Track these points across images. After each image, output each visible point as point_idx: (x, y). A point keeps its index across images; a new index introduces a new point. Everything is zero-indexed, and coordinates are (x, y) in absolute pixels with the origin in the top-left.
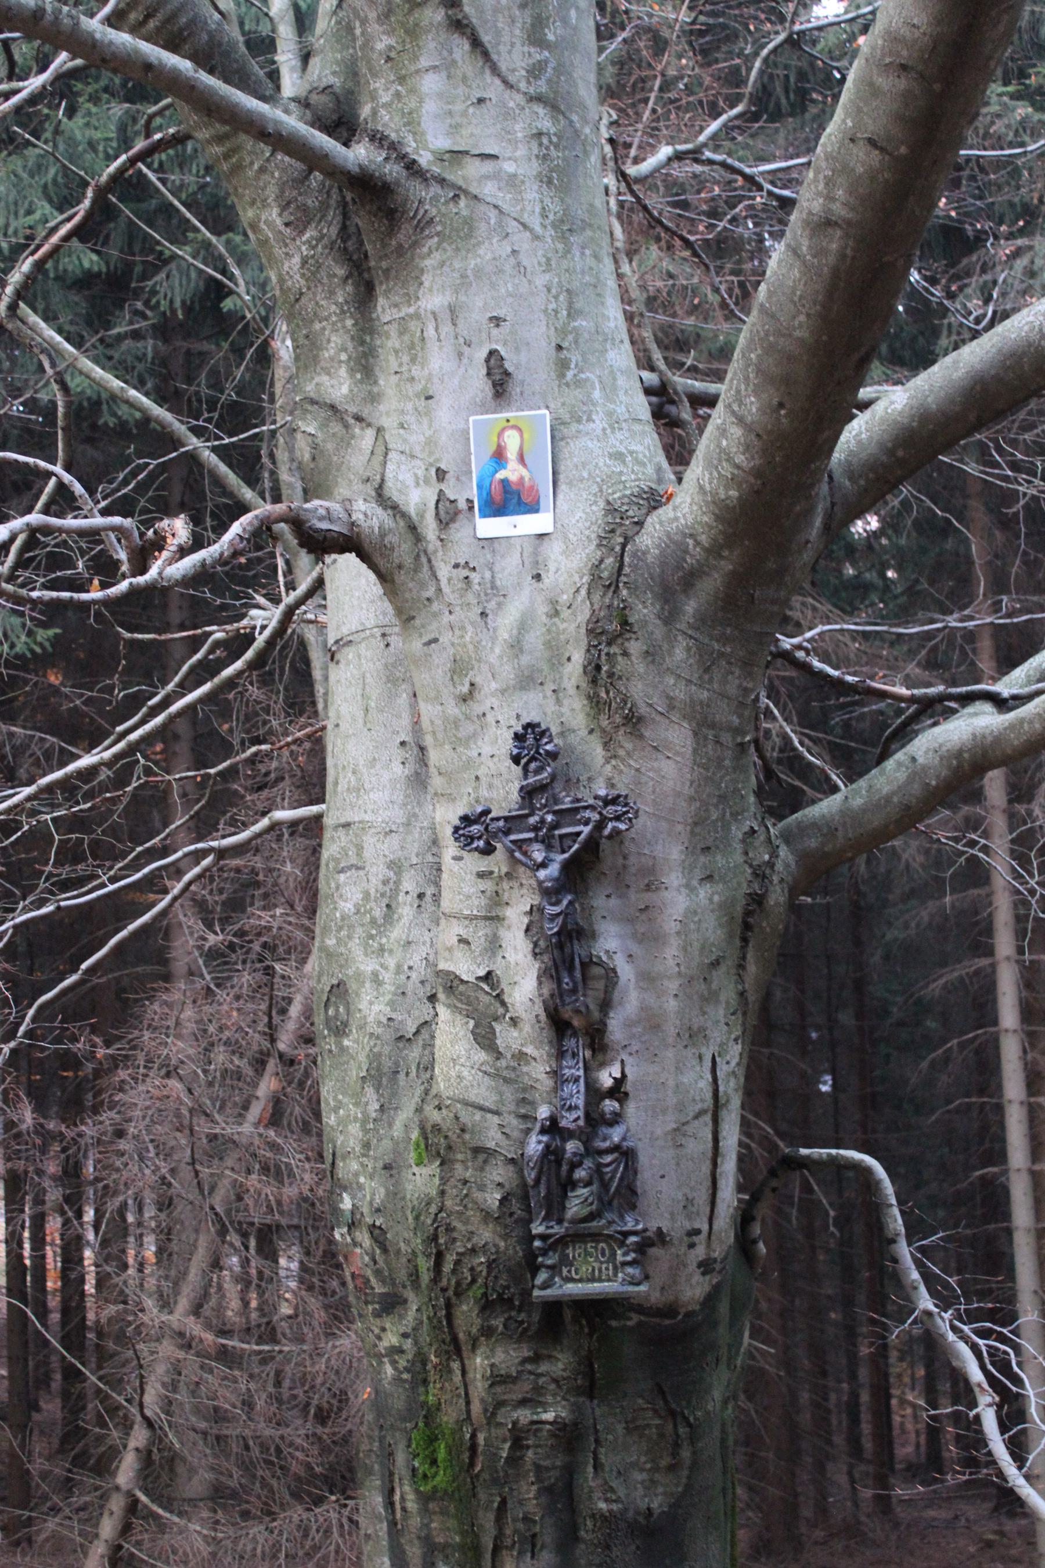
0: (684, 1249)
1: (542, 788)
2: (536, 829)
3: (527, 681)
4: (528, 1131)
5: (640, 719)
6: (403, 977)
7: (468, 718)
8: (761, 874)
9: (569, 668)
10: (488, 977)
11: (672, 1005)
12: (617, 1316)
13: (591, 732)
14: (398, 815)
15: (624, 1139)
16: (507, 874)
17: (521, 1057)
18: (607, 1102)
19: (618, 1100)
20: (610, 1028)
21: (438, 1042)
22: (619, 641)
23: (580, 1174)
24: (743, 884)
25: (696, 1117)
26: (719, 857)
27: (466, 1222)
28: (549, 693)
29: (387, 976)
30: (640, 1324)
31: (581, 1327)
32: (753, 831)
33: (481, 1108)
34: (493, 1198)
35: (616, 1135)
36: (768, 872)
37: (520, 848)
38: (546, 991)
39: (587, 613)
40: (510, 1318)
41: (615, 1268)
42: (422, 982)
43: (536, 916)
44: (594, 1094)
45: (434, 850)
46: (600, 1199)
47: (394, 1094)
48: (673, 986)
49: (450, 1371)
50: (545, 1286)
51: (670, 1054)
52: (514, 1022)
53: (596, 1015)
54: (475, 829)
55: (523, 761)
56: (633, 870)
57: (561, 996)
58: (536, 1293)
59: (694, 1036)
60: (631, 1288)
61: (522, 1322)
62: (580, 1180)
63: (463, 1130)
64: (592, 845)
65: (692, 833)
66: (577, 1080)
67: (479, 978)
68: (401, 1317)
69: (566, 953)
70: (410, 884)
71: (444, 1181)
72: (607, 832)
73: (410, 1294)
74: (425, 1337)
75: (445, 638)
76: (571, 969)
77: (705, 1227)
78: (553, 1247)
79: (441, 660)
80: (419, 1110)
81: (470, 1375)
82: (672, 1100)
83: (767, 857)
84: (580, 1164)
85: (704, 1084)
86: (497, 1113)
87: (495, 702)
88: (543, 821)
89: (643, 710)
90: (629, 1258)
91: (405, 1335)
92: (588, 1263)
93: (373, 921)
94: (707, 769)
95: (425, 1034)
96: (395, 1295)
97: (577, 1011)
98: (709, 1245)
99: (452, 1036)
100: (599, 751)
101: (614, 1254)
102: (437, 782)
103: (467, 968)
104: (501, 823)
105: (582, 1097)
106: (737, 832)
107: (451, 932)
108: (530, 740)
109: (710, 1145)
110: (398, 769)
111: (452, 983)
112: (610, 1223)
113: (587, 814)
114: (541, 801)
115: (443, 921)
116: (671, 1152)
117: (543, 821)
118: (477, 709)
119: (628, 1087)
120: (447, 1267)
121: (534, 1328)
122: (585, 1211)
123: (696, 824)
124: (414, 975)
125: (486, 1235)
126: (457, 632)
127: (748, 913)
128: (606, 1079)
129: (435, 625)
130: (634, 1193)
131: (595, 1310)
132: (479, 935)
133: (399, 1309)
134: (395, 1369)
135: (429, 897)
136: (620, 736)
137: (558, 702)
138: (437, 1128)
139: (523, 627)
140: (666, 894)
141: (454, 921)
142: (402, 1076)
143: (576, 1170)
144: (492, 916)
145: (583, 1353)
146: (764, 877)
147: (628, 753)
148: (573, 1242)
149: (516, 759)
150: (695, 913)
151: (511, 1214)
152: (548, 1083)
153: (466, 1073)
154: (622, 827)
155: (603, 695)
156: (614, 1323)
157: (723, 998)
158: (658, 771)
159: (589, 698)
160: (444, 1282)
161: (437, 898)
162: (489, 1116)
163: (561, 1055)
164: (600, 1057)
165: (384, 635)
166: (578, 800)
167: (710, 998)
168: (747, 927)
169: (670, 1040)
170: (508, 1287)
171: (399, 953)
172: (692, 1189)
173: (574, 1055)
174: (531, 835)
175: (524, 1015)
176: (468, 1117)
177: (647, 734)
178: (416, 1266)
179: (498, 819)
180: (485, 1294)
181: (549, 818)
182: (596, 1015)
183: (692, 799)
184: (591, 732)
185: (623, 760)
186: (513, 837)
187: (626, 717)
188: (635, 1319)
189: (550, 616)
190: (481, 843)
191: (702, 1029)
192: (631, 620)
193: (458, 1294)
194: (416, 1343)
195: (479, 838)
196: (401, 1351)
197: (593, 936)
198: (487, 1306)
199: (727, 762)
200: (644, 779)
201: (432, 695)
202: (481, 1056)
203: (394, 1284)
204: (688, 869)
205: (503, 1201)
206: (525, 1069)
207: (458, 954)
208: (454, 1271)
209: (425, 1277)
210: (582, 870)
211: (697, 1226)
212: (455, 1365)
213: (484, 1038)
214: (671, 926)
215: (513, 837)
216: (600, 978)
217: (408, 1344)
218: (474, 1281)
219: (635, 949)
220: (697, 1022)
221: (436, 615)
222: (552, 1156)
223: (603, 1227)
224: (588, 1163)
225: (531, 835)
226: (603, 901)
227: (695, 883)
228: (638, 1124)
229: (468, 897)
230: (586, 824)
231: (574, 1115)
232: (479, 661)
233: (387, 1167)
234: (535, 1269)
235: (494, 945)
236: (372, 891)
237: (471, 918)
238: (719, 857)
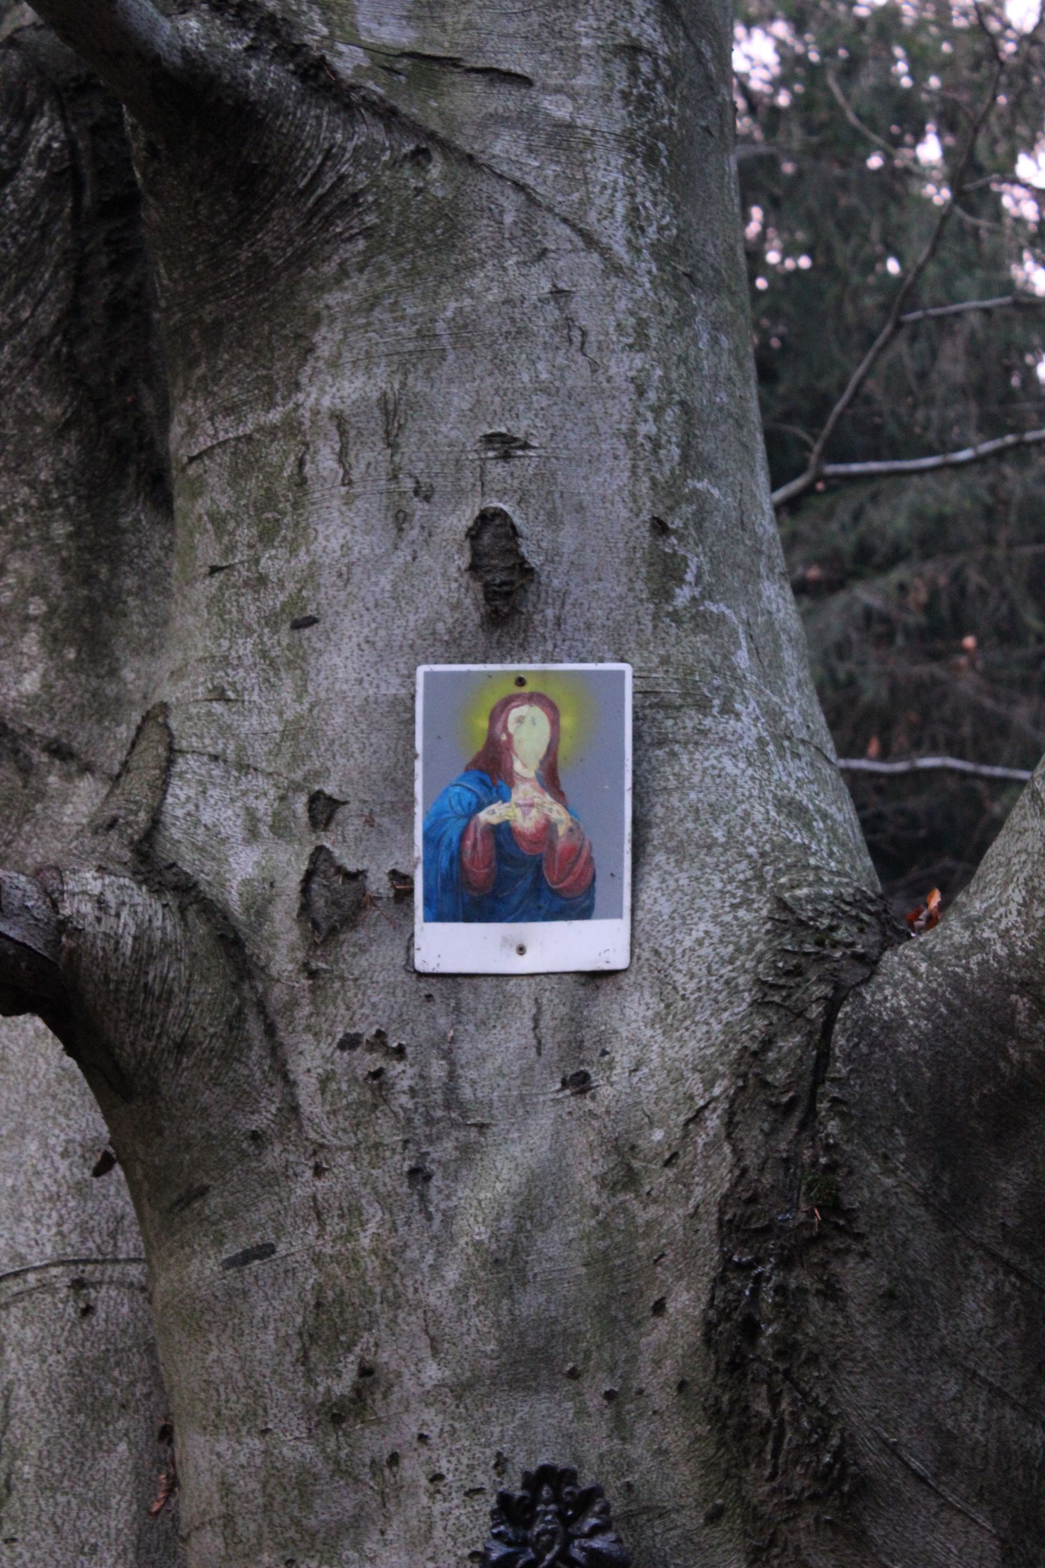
3: (531, 1363)
5: (864, 1485)
7: (342, 1469)
9: (659, 1332)
13: (714, 1517)
22: (816, 1255)
28: (594, 1402)
39: (724, 1175)
75: (294, 1246)
79: (275, 1309)
87: (433, 1420)
89: (872, 1459)
118: (374, 1444)
126: (335, 1226)
129: (267, 1207)
137: (621, 1428)
139: (530, 1210)
155: (761, 1407)
159: (716, 1415)
165: (78, 1285)
177: (876, 1533)
187: (822, 1476)
189: (609, 1185)
192: (850, 1200)
201: (237, 1405)
221: (271, 1181)
232: (395, 1303)
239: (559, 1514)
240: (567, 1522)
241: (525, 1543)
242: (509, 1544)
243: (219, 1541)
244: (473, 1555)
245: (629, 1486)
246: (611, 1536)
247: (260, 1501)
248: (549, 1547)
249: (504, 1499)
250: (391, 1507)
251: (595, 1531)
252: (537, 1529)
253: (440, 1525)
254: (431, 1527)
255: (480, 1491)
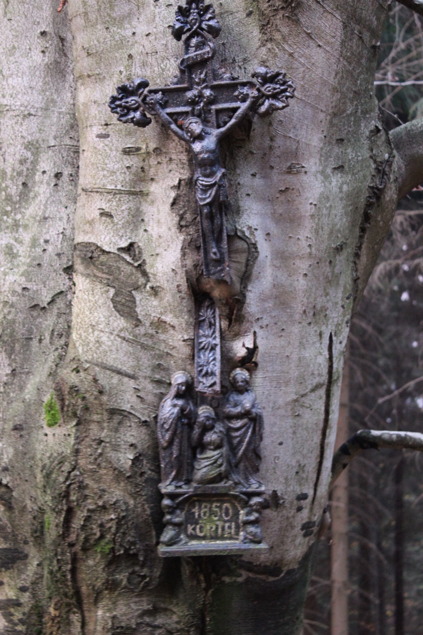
0: (293, 511)
1: (202, 63)
2: (193, 103)
4: (161, 396)
6: (39, 250)
8: (382, 170)
10: (130, 248)
11: (301, 283)
12: (231, 573)
13: (249, 14)
14: (36, 100)
15: (253, 406)
16: (155, 150)
17: (159, 325)
18: (238, 371)
19: (248, 370)
20: (248, 301)
21: (75, 310)
23: (211, 437)
24: (366, 178)
25: (313, 390)
26: (349, 150)
27: (98, 481)
29: (21, 250)
30: (248, 580)
31: (199, 582)
32: (377, 130)
33: (119, 372)
34: (126, 458)
35: (246, 401)
36: (387, 169)
37: (176, 122)
38: (189, 262)
40: (133, 573)
41: (238, 527)
42: (59, 255)
43: (184, 190)
44: (229, 363)
45: (72, 134)
46: (229, 462)
47: (26, 360)
48: (303, 266)
49: (69, 623)
50: (170, 543)
51: (296, 329)
52: (155, 291)
53: (238, 286)
54: (132, 100)
55: (184, 37)
56: (278, 152)
57: (207, 266)
58: (162, 549)
59: (317, 314)
60: (252, 546)
61: (144, 577)
62: (210, 443)
63: (101, 392)
64: (245, 124)
65: (331, 122)
66: (213, 348)
67: (120, 249)
68: (20, 572)
69: (211, 226)
70: (47, 164)
71: (79, 440)
72: (263, 109)
73: (32, 550)
74: (44, 591)
76: (218, 241)
77: (311, 493)
78: (180, 506)
80: (52, 374)
81: (90, 627)
82: (294, 373)
83: (387, 156)
84: (212, 427)
85: (322, 360)
86: (132, 377)
88: (201, 95)
90: (252, 518)
91: (23, 589)
92: (212, 521)
93: (9, 199)
94: (350, 63)
95: (60, 303)
96: (16, 550)
97: (221, 282)
98: (311, 509)
99: (90, 304)
100: (256, 33)
101: (237, 514)
102: (82, 64)
103: (109, 239)
104: (159, 96)
105: (218, 364)
106: (365, 129)
107: (91, 208)
108: (193, 15)
109: (322, 417)
110: (37, 58)
111: (92, 255)
112: (236, 484)
113: (245, 90)
114: (199, 76)
115: (83, 198)
116: (290, 421)
117: (201, 95)
119: (258, 358)
120: (77, 523)
121: (155, 582)
122: (214, 472)
123: (335, 115)
124: (50, 248)
125: (117, 493)
127: (369, 205)
128: (239, 349)
130: (258, 457)
131: (212, 565)
132: (122, 208)
133: (19, 564)
134: (10, 621)
135: (67, 176)
136: (278, 20)
138: (74, 390)
140: (305, 178)
141: (97, 196)
142: (35, 343)
143: (206, 433)
144: (137, 190)
145: (198, 607)
146: (384, 173)
147: (284, 38)
148: (200, 502)
149: (177, 34)
150: (327, 199)
151: (142, 474)
152: (186, 350)
153: (104, 339)
154: (280, 104)
156: (227, 579)
157: (342, 282)
158: (308, 58)
160: (73, 537)
161: (74, 178)
162: (126, 379)
163: (198, 324)
164: (236, 328)
166: (234, 79)
167: (331, 281)
168: (367, 217)
169: (297, 317)
170: (133, 543)
171: (34, 229)
172: (304, 457)
173: (211, 325)
174: (188, 109)
175: (165, 285)
176: (107, 380)
177: (302, 20)
178: (42, 524)
179: (156, 92)
180: (113, 550)
181: (207, 93)
182: (238, 286)
183: (335, 90)
184: (249, 14)
185: (278, 44)
186: (169, 110)
188: (244, 576)
190: (138, 115)
191: (324, 309)
193: (85, 549)
194: (34, 596)
195: (135, 110)
196: (17, 604)
197: (238, 211)
198: (113, 561)
199: (363, 61)
200: (296, 65)
202: (121, 323)
203: (15, 541)
204: (325, 157)
205: (136, 460)
206: (162, 337)
207: (100, 227)
208: (83, 527)
209: (52, 533)
210: (233, 146)
211: (305, 491)
212: (75, 618)
213: (125, 306)
214: (307, 209)
215: (169, 110)
216: (243, 252)
217: (25, 598)
218: (102, 537)
219: (274, 229)
220: (320, 302)
222: (185, 419)
223: (230, 488)
224: (219, 427)
225: (188, 109)
226: (249, 180)
227: (329, 171)
228: (263, 394)
229: (113, 173)
230: (243, 100)
231: (209, 381)
233: (16, 428)
234: (160, 527)
235: (137, 219)
236: (9, 171)
237: (115, 193)
238: (349, 150)
239: (198, 13)
240: (201, 16)
241: (187, 23)
242: (182, 23)
243: (83, 21)
244: (169, 26)
245: (221, 4)
246: (215, 21)
247: (97, 8)
248: (195, 24)
249: (180, 8)
250: (141, 10)
251: (210, 19)
252: (191, 18)
253: (158, 16)
254: (155, 17)
255: (171, 5)
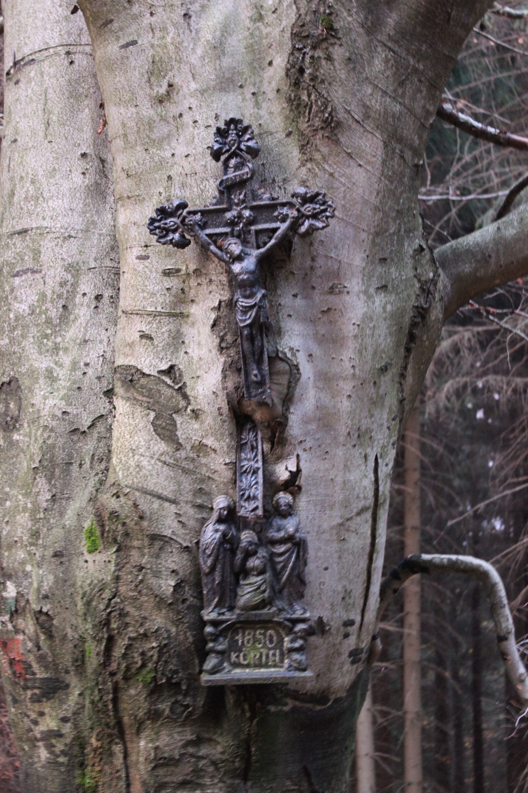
0: (340, 638)
1: (241, 184)
2: (232, 223)
3: (227, 82)
4: (203, 522)
5: (339, 124)
6: (79, 373)
7: (163, 119)
8: (426, 289)
9: (270, 72)
10: (170, 371)
11: (345, 405)
12: (276, 702)
13: (289, 134)
14: (77, 222)
15: (297, 530)
16: (195, 271)
17: (201, 448)
18: (281, 494)
19: (292, 494)
20: (290, 423)
21: (115, 434)
22: (324, 45)
23: (254, 562)
24: (411, 297)
25: (359, 514)
26: (393, 270)
27: (139, 608)
28: (249, 96)
29: (61, 373)
30: (294, 710)
31: (243, 712)
32: (422, 249)
33: (160, 497)
34: (167, 585)
35: (290, 525)
36: (432, 288)
37: (215, 243)
38: (230, 385)
39: (293, 17)
40: (176, 702)
41: (282, 655)
42: (99, 378)
43: (224, 311)
44: (271, 486)
45: (113, 255)
46: (272, 588)
47: (66, 485)
48: (347, 387)
49: (111, 754)
50: (214, 671)
51: (340, 452)
52: (196, 414)
53: (279, 408)
54: (171, 221)
55: (223, 158)
56: (319, 272)
57: (248, 388)
58: (205, 677)
59: (362, 436)
60: (297, 674)
61: (187, 706)
62: (253, 569)
63: (141, 518)
64: (285, 244)
65: (373, 241)
66: (255, 472)
67: (160, 372)
68: (62, 702)
69: (252, 347)
70: (87, 286)
71: (119, 566)
72: (303, 229)
73: (73, 680)
74: (86, 722)
75: (145, 40)
76: (259, 362)
77: (358, 619)
78: (223, 633)
79: (139, 62)
80: (92, 500)
81: (133, 758)
82: (339, 496)
83: (431, 275)
84: (255, 553)
85: (368, 482)
86: (173, 502)
87: (194, 102)
88: (240, 216)
89: (341, 115)
90: (297, 645)
91: (64, 720)
92: (256, 649)
93: (49, 321)
94: (392, 182)
95: (101, 427)
96: (57, 680)
97: (262, 404)
98: (359, 636)
99: (131, 428)
100: (296, 153)
101: (281, 641)
102: (122, 185)
103: (149, 362)
104: (198, 217)
105: (260, 488)
106: (409, 248)
107: (131, 330)
108: (232, 136)
109: (369, 541)
110: (78, 179)
111: (132, 378)
112: (280, 610)
113: (285, 211)
114: (238, 197)
115: (123, 320)
116: (335, 546)
117: (240, 216)
118: (173, 110)
119: (302, 481)
120: (118, 651)
121: (199, 712)
122: (258, 598)
123: (377, 234)
124: (90, 371)
125: (159, 620)
126: (158, 34)
127: (414, 325)
128: (282, 472)
129: (134, 27)
130: (303, 582)
131: (258, 695)
132: (162, 330)
133: (60, 694)
134: (52, 753)
135: (107, 299)
136: (318, 140)
137: (257, 105)
138: (114, 515)
139: (226, 30)
140: (347, 298)
141: (137, 318)
142: (75, 467)
144: (177, 312)
145: (243, 737)
146: (429, 292)
147: (324, 158)
148: (244, 629)
149: (216, 155)
150: (371, 319)
151: (184, 601)
152: (228, 474)
153: (145, 463)
154: (320, 224)
155: (305, 98)
156: (272, 708)
157: (387, 403)
158: (349, 178)
159: (289, 100)
160: (114, 666)
161: (114, 300)
162: (167, 504)
163: (240, 447)
164: (278, 451)
165: (68, 53)
166: (273, 199)
167: (376, 402)
168: (412, 337)
169: (341, 439)
170: (176, 672)
171: (75, 352)
172: (351, 582)
173: (253, 448)
174: (227, 230)
175: (206, 408)
176: (146, 505)
177: (342, 140)
178: (83, 653)
179: (195, 213)
180: (154, 679)
181: (247, 213)
182: (279, 408)
183: (376, 209)
184: (289, 134)
185: (318, 164)
186: (208, 231)
187: (325, 121)
188: (290, 704)
189: (254, 20)
190: (177, 236)
191: (369, 431)
192: (336, 26)
193: (126, 678)
194: (76, 726)
195: (174, 231)
196: (59, 735)
197: (279, 333)
198: (155, 690)
199: (406, 180)
200: (337, 184)
201: (127, 97)
202: (161, 446)
203: (56, 670)
204: (368, 276)
205: (177, 587)
206: (204, 460)
207: (140, 349)
208: (124, 656)
209: (93, 662)
210: (273, 267)
211: (352, 617)
212: (117, 749)
213: (165, 429)
214: (350, 330)
215: (208, 231)
216: (284, 373)
217: (67, 729)
218: (144, 666)
219: (317, 351)
220: (365, 423)
221: (135, 17)
222: (227, 544)
223: (274, 615)
224: (262, 552)
225: (227, 230)
226: (290, 300)
227: (372, 290)
228: (307, 517)
229: (153, 294)
230: (283, 220)
231: (252, 505)
232: (180, 62)
233: (57, 555)
234: (203, 655)
235: (177, 341)
236: (49, 293)
237: (155, 315)
238: (393, 270)
239: (237, 134)
240: (239, 137)
241: (225, 144)
242: (220, 144)
243: (122, 143)
244: (208, 148)
245: (260, 125)
246: (254, 141)
247: (136, 129)
248: (233, 145)
249: (218, 129)
250: (180, 131)
251: (249, 140)
252: (229, 139)
253: (197, 137)
254: (194, 138)
255: (210, 126)
